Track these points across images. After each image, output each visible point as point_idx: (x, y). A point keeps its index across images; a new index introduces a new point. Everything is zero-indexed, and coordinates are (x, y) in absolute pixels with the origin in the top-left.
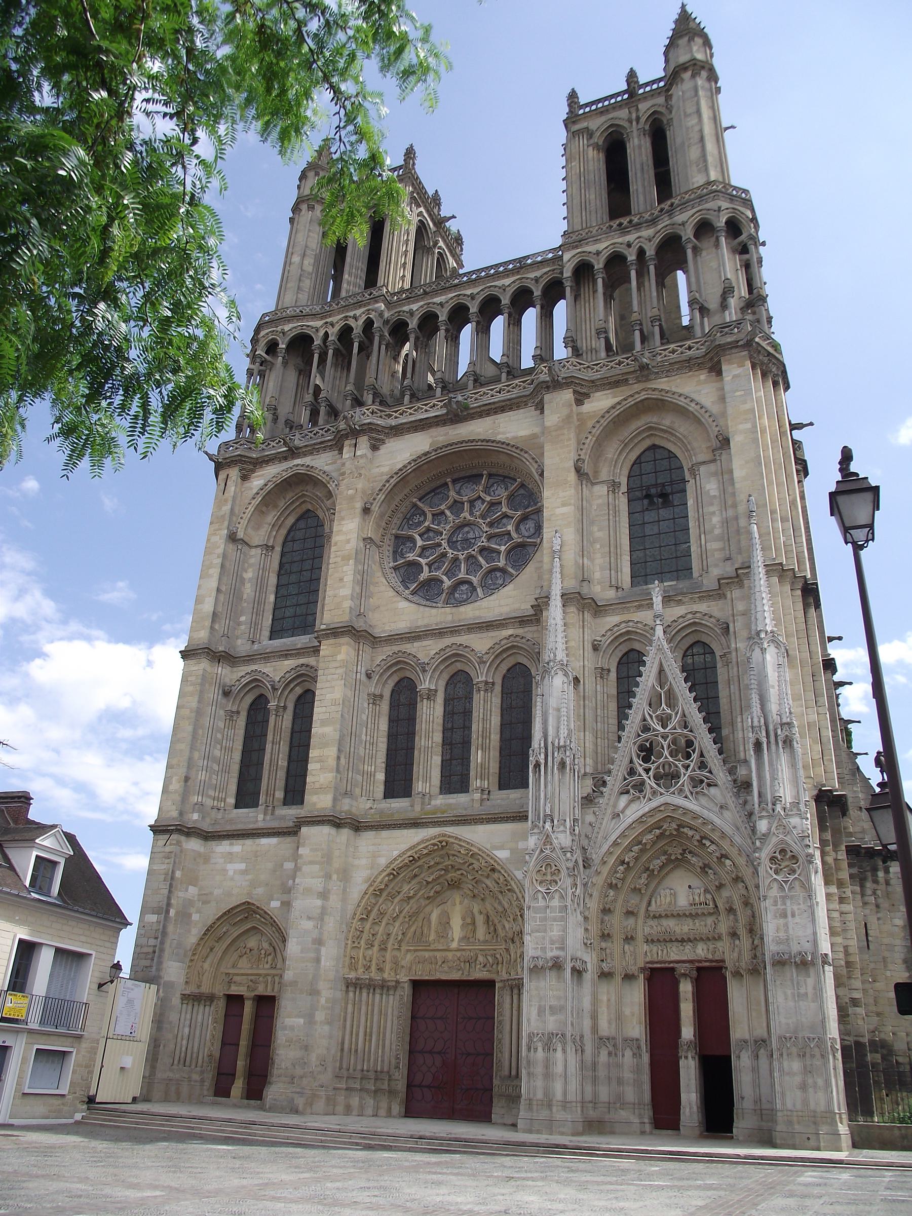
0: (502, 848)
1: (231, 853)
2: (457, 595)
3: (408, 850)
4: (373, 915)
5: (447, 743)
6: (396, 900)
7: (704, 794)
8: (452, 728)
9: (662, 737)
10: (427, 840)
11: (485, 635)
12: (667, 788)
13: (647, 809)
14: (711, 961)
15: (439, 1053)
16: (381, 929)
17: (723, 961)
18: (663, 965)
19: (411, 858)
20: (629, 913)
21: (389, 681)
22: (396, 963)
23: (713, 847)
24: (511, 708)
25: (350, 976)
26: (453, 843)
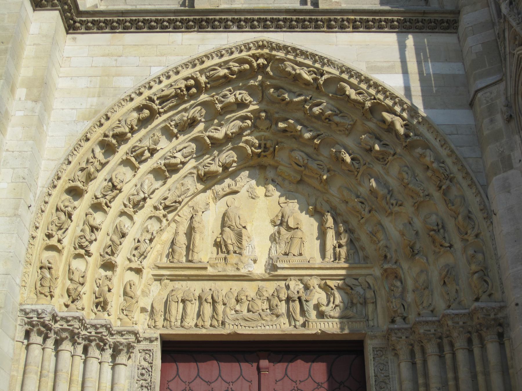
3: (186, 65)
6: (144, 168)
16: (106, 221)
19: (192, 82)
25: (39, 308)
26: (282, 61)
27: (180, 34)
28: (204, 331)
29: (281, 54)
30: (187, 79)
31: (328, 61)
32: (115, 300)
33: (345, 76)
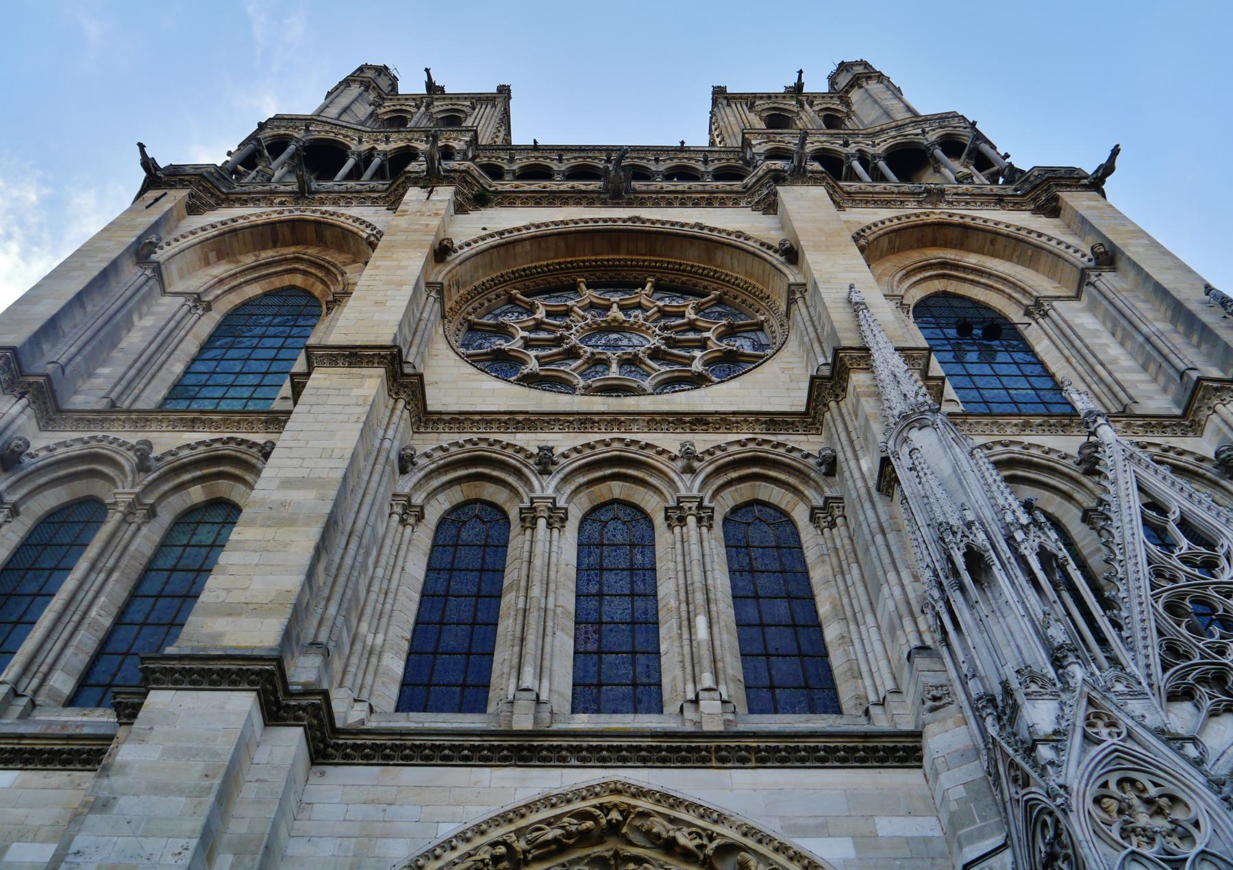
0: (822, 829)
3: (496, 821)
5: (588, 622)
8: (600, 595)
19: (502, 850)
21: (441, 497)
24: (752, 571)
26: (645, 815)
27: (487, 770)
29: (644, 804)
30: (494, 844)
31: (720, 815)
33: (750, 842)
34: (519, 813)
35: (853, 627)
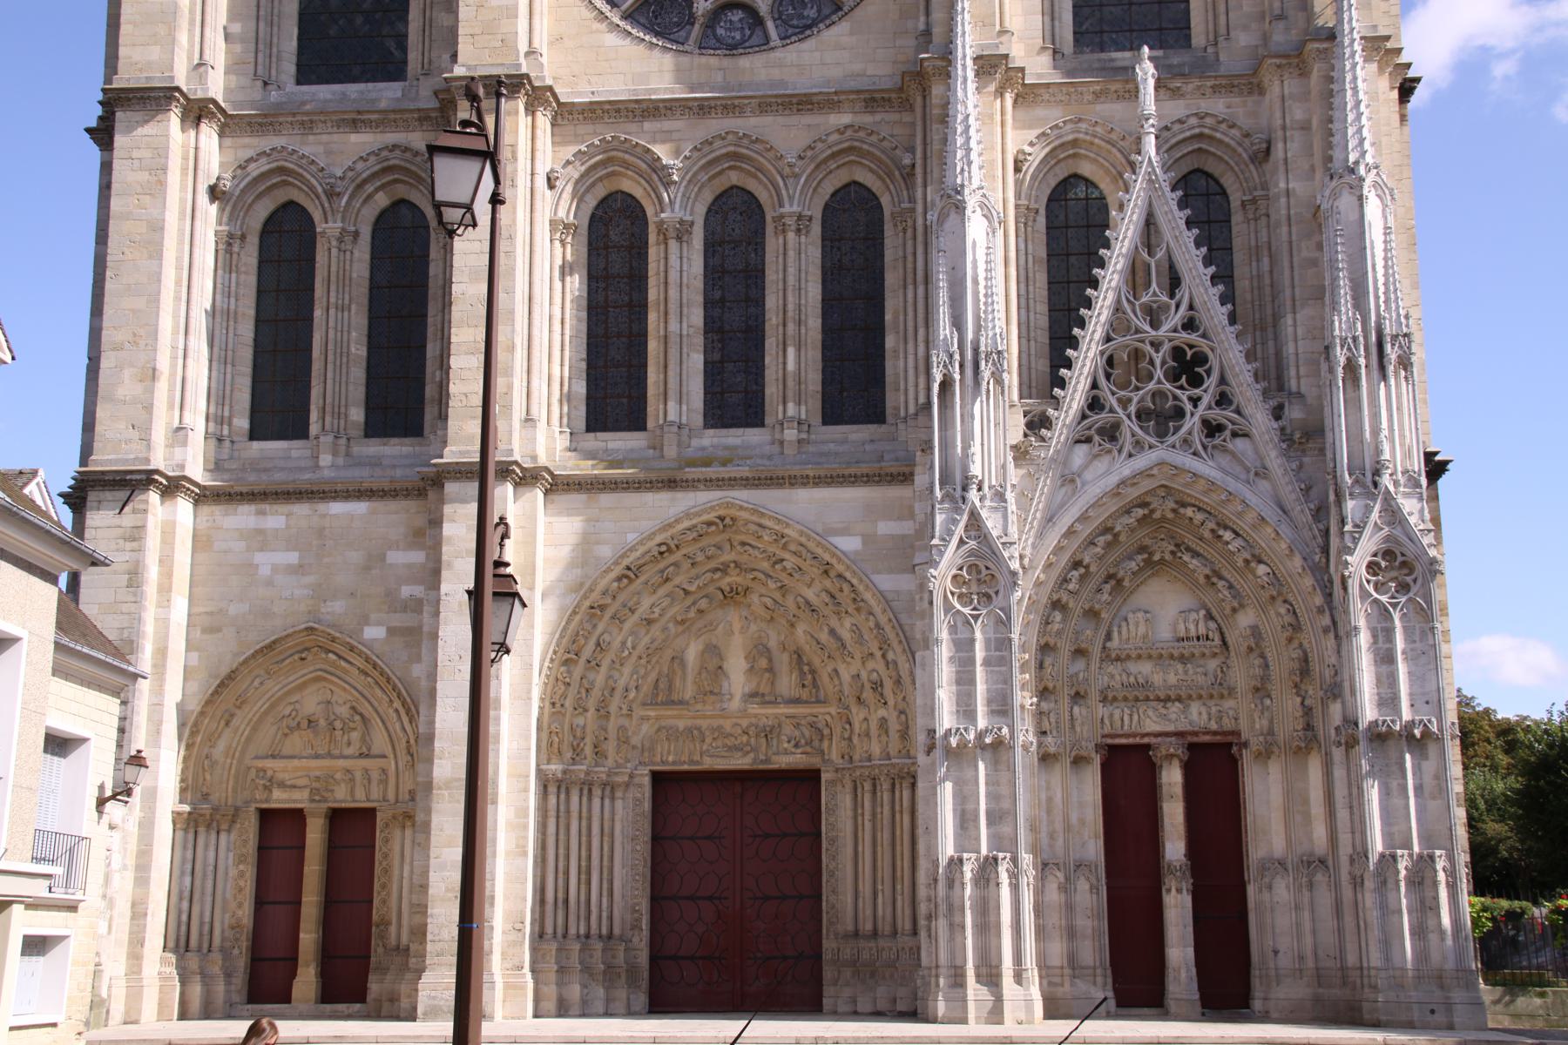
0: (845, 531)
1: (260, 532)
2: (720, 31)
4: (587, 652)
6: (627, 626)
7: (1225, 450)
8: (722, 300)
9: (1152, 344)
10: (698, 514)
11: (795, 119)
12: (1161, 434)
13: (1127, 472)
14: (1215, 733)
15: (710, 898)
16: (600, 678)
17: (1237, 733)
18: (1131, 741)
19: (664, 548)
20: (1079, 652)
22: (623, 740)
23: (1238, 543)
28: (686, 767)
29: (745, 515)
30: (660, 545)
32: (610, 747)
34: (670, 526)
35: (902, 346)
